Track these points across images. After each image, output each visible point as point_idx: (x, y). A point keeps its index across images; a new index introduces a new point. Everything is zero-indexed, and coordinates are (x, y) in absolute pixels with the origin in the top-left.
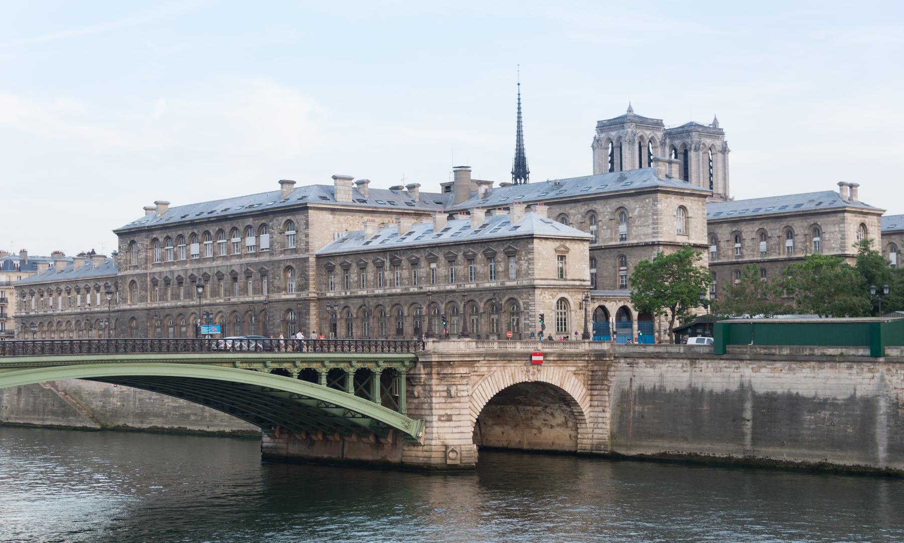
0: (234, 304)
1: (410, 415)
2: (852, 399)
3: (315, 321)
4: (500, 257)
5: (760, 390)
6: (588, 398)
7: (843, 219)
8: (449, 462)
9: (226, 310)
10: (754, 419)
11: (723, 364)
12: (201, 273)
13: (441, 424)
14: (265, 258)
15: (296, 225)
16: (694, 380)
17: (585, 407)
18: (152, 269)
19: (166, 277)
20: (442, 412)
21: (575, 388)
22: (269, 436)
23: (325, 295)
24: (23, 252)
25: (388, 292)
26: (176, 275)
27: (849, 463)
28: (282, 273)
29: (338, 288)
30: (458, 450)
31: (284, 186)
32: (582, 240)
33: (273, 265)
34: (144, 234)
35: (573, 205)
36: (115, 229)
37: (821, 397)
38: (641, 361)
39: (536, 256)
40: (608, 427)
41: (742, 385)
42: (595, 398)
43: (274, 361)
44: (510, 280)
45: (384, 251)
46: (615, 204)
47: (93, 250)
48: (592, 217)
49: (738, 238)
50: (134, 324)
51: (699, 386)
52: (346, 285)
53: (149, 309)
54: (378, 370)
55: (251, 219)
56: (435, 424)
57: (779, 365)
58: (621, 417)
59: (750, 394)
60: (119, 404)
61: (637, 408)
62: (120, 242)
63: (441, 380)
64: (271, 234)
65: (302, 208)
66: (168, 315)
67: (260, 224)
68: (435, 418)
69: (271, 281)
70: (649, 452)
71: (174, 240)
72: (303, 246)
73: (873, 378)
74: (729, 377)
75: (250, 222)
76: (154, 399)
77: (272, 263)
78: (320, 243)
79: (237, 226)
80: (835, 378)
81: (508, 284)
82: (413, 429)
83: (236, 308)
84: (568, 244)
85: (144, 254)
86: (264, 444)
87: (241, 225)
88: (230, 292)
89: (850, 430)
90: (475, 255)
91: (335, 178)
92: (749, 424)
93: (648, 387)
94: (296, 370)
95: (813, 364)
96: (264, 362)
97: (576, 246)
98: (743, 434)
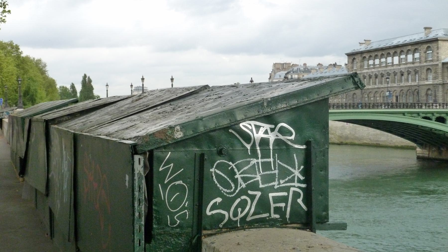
3: (441, 94)
9: (399, 90)
12: (386, 72)
14: (416, 65)
15: (432, 48)
18: (363, 71)
19: (370, 74)
22: (420, 148)
23: (447, 82)
24: (305, 64)
26: (374, 73)
28: (425, 72)
31: (426, 30)
33: (421, 68)
34: (359, 55)
36: (346, 53)
43: (423, 113)
47: (336, 63)
50: (355, 96)
55: (410, 46)
60: (349, 132)
62: (349, 59)
64: (420, 53)
65: (436, 40)
66: (370, 92)
67: (414, 48)
69: (420, 75)
71: (373, 57)
72: (435, 58)
75: (409, 47)
76: (365, 130)
77: (421, 67)
78: (444, 57)
79: (403, 50)
83: (403, 88)
85: (360, 64)
86: (418, 152)
87: (405, 49)
88: (401, 81)
96: (418, 114)
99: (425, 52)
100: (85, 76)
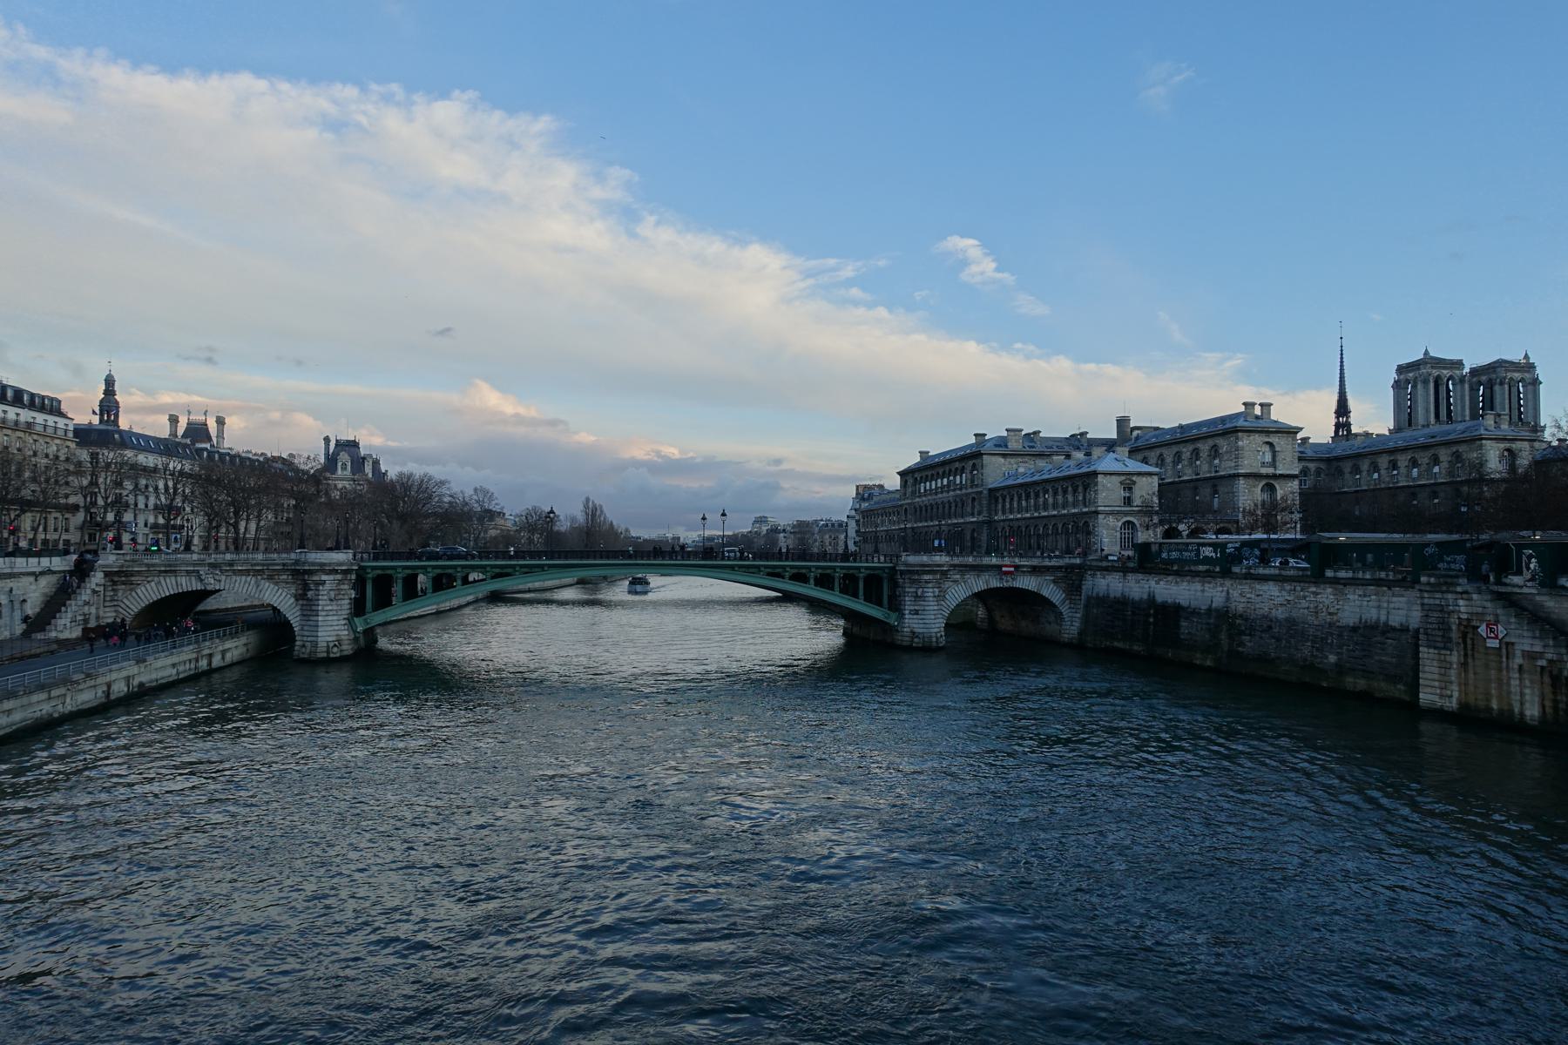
0: (949, 525)
1: (890, 609)
4: (1080, 489)
5: (1159, 599)
6: (1068, 602)
7: (1481, 445)
11: (1140, 576)
17: (1064, 609)
20: (912, 608)
21: (1052, 592)
30: (921, 636)
32: (1150, 474)
37: (1193, 606)
39: (1100, 487)
40: (1077, 624)
41: (1149, 595)
43: (766, 567)
44: (1086, 506)
45: (1021, 485)
46: (1211, 442)
48: (1197, 454)
49: (1394, 465)
52: (1004, 513)
53: (913, 528)
57: (1170, 578)
68: (907, 612)
73: (1222, 591)
75: (957, 465)
81: (1085, 510)
82: (892, 620)
93: (1101, 595)
95: (1188, 578)
96: (758, 567)
99: (971, 472)
100: (588, 500)
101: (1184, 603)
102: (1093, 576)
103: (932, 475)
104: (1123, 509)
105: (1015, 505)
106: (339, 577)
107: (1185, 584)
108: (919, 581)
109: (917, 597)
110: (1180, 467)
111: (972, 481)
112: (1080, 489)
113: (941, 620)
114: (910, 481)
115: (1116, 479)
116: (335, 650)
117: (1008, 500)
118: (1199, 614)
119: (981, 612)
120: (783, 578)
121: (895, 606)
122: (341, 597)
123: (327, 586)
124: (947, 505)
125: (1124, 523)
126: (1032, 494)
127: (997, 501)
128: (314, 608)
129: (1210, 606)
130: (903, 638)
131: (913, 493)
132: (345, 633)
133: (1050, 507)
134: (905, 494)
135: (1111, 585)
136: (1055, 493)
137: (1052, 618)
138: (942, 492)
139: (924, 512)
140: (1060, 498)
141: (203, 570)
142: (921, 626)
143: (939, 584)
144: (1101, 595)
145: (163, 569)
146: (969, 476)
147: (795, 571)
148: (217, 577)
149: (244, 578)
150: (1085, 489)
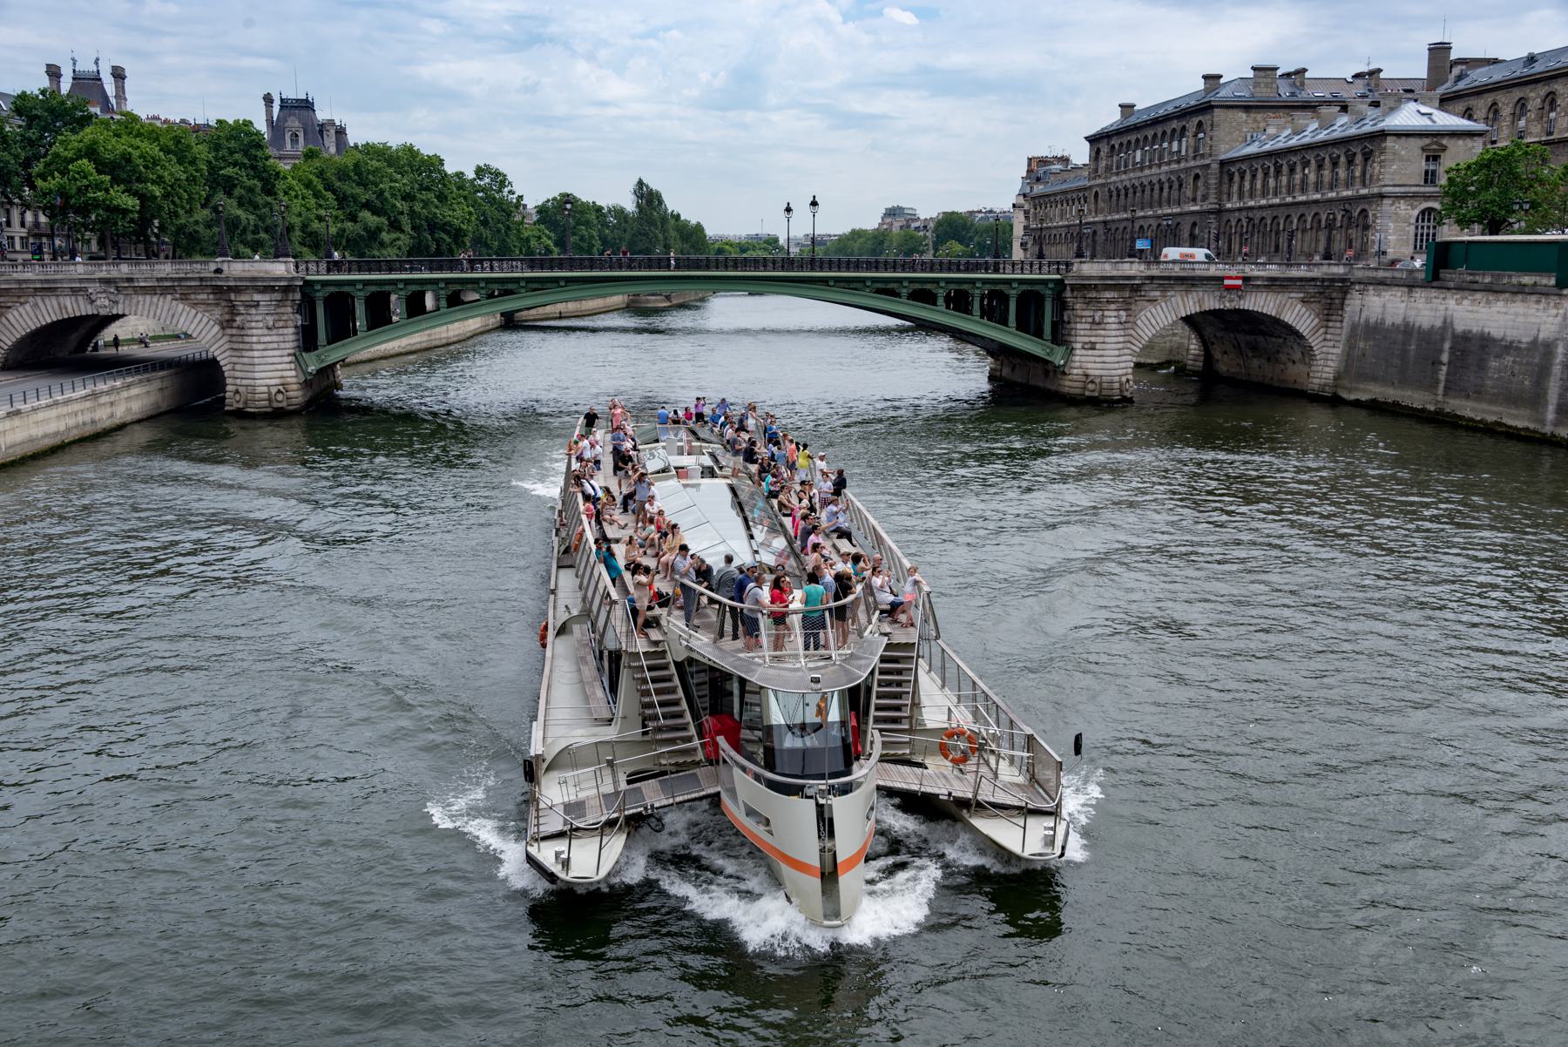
0: (1158, 217)
2: (1534, 343)
4: (1359, 159)
6: (1322, 330)
8: (1087, 393)
10: (1450, 363)
11: (1434, 293)
13: (1084, 352)
16: (1412, 313)
17: (1315, 342)
20: (1086, 339)
21: (1297, 314)
25: (1270, 202)
27: (1520, 424)
29: (1235, 197)
30: (1097, 381)
32: (1470, 134)
35: (1533, 86)
37: (1509, 339)
38: (1371, 288)
41: (1445, 319)
42: (1330, 330)
43: (874, 280)
44: (1364, 186)
45: (1269, 155)
48: (1553, 102)
51: (1411, 320)
52: (1241, 197)
53: (1105, 223)
54: (1014, 292)
56: (1078, 352)
57: (1478, 296)
58: (1348, 354)
59: (1450, 331)
61: (1362, 345)
63: (1088, 304)
68: (1079, 346)
70: (1364, 397)
74: (1436, 310)
75: (1175, 124)
80: (1524, 315)
81: (1364, 191)
84: (1444, 142)
89: (1527, 383)
90: (1339, 156)
91: (1254, 69)
92: (1445, 368)
93: (1372, 320)
94: (905, 291)
95: (1507, 295)
97: (1461, 142)
98: (1438, 381)
99: (1195, 135)
100: (640, 183)
101: (1496, 333)
102: (1361, 292)
103: (1137, 140)
104: (1422, 189)
105: (1259, 185)
106: (277, 296)
107: (1501, 304)
108: (1097, 300)
109: (1097, 324)
110: (1522, 123)
111: (1196, 149)
112: (1359, 159)
113: (1129, 358)
114: (1105, 149)
115: (1416, 144)
116: (280, 397)
117: (1248, 177)
118: (1518, 349)
119: (1194, 347)
120: (898, 295)
121: (1060, 337)
122: (281, 324)
123: (262, 310)
124: (1157, 187)
125: (1423, 212)
126: (1285, 169)
127: (1231, 179)
128: (247, 339)
129: (1536, 339)
130: (1070, 385)
131: (1108, 168)
132: (291, 375)
133: (1311, 187)
134: (1096, 170)
135: (1389, 305)
136: (1320, 167)
137: (1297, 356)
138: (1150, 167)
139: (1122, 197)
140: (1326, 173)
141: (92, 288)
142: (1099, 366)
143: (1127, 306)
144: (1372, 320)
145: (38, 286)
146: (1192, 141)
147: (918, 286)
148: (112, 297)
149: (148, 297)
150: (1366, 160)
